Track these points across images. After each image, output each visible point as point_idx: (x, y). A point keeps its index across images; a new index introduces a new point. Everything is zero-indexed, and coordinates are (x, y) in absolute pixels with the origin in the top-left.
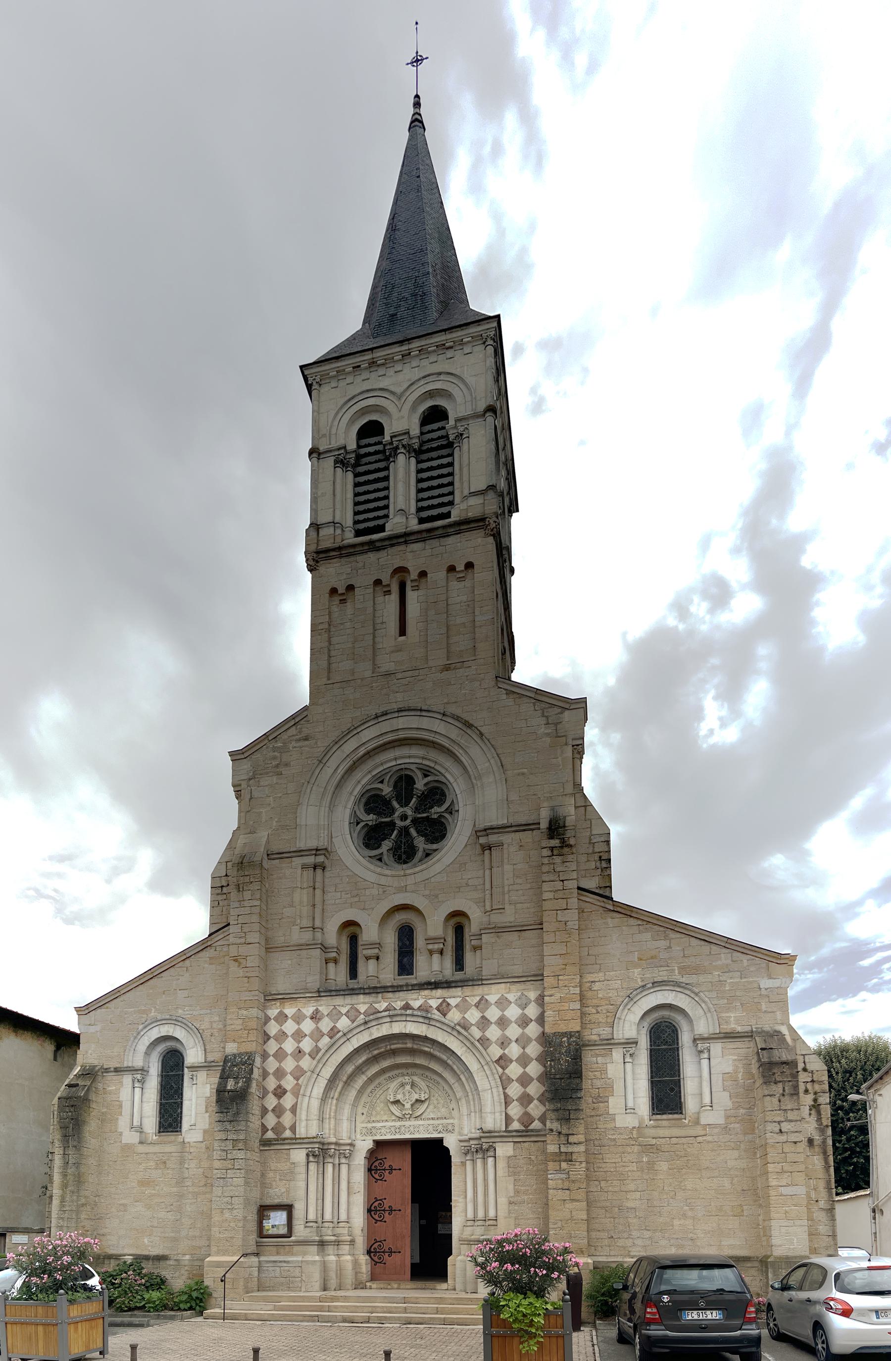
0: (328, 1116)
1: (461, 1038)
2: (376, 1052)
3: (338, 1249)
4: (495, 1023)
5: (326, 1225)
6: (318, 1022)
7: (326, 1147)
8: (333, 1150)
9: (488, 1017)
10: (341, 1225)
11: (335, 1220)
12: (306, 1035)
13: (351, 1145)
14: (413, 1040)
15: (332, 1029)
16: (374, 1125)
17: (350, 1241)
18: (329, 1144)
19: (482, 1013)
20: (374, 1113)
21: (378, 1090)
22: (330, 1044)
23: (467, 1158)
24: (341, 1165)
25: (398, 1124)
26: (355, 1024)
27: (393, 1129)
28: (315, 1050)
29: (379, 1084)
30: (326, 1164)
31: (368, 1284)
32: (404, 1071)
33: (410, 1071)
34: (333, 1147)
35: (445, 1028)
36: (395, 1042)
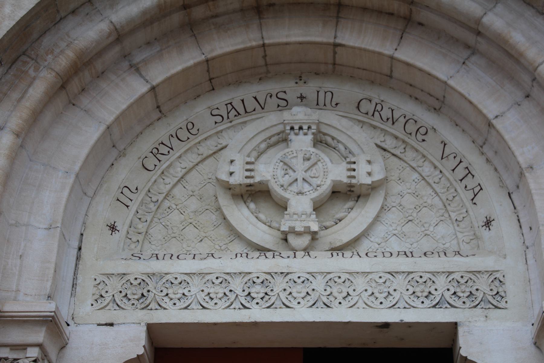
16: (156, 266)
20: (157, 232)
21: (180, 148)
27: (237, 285)
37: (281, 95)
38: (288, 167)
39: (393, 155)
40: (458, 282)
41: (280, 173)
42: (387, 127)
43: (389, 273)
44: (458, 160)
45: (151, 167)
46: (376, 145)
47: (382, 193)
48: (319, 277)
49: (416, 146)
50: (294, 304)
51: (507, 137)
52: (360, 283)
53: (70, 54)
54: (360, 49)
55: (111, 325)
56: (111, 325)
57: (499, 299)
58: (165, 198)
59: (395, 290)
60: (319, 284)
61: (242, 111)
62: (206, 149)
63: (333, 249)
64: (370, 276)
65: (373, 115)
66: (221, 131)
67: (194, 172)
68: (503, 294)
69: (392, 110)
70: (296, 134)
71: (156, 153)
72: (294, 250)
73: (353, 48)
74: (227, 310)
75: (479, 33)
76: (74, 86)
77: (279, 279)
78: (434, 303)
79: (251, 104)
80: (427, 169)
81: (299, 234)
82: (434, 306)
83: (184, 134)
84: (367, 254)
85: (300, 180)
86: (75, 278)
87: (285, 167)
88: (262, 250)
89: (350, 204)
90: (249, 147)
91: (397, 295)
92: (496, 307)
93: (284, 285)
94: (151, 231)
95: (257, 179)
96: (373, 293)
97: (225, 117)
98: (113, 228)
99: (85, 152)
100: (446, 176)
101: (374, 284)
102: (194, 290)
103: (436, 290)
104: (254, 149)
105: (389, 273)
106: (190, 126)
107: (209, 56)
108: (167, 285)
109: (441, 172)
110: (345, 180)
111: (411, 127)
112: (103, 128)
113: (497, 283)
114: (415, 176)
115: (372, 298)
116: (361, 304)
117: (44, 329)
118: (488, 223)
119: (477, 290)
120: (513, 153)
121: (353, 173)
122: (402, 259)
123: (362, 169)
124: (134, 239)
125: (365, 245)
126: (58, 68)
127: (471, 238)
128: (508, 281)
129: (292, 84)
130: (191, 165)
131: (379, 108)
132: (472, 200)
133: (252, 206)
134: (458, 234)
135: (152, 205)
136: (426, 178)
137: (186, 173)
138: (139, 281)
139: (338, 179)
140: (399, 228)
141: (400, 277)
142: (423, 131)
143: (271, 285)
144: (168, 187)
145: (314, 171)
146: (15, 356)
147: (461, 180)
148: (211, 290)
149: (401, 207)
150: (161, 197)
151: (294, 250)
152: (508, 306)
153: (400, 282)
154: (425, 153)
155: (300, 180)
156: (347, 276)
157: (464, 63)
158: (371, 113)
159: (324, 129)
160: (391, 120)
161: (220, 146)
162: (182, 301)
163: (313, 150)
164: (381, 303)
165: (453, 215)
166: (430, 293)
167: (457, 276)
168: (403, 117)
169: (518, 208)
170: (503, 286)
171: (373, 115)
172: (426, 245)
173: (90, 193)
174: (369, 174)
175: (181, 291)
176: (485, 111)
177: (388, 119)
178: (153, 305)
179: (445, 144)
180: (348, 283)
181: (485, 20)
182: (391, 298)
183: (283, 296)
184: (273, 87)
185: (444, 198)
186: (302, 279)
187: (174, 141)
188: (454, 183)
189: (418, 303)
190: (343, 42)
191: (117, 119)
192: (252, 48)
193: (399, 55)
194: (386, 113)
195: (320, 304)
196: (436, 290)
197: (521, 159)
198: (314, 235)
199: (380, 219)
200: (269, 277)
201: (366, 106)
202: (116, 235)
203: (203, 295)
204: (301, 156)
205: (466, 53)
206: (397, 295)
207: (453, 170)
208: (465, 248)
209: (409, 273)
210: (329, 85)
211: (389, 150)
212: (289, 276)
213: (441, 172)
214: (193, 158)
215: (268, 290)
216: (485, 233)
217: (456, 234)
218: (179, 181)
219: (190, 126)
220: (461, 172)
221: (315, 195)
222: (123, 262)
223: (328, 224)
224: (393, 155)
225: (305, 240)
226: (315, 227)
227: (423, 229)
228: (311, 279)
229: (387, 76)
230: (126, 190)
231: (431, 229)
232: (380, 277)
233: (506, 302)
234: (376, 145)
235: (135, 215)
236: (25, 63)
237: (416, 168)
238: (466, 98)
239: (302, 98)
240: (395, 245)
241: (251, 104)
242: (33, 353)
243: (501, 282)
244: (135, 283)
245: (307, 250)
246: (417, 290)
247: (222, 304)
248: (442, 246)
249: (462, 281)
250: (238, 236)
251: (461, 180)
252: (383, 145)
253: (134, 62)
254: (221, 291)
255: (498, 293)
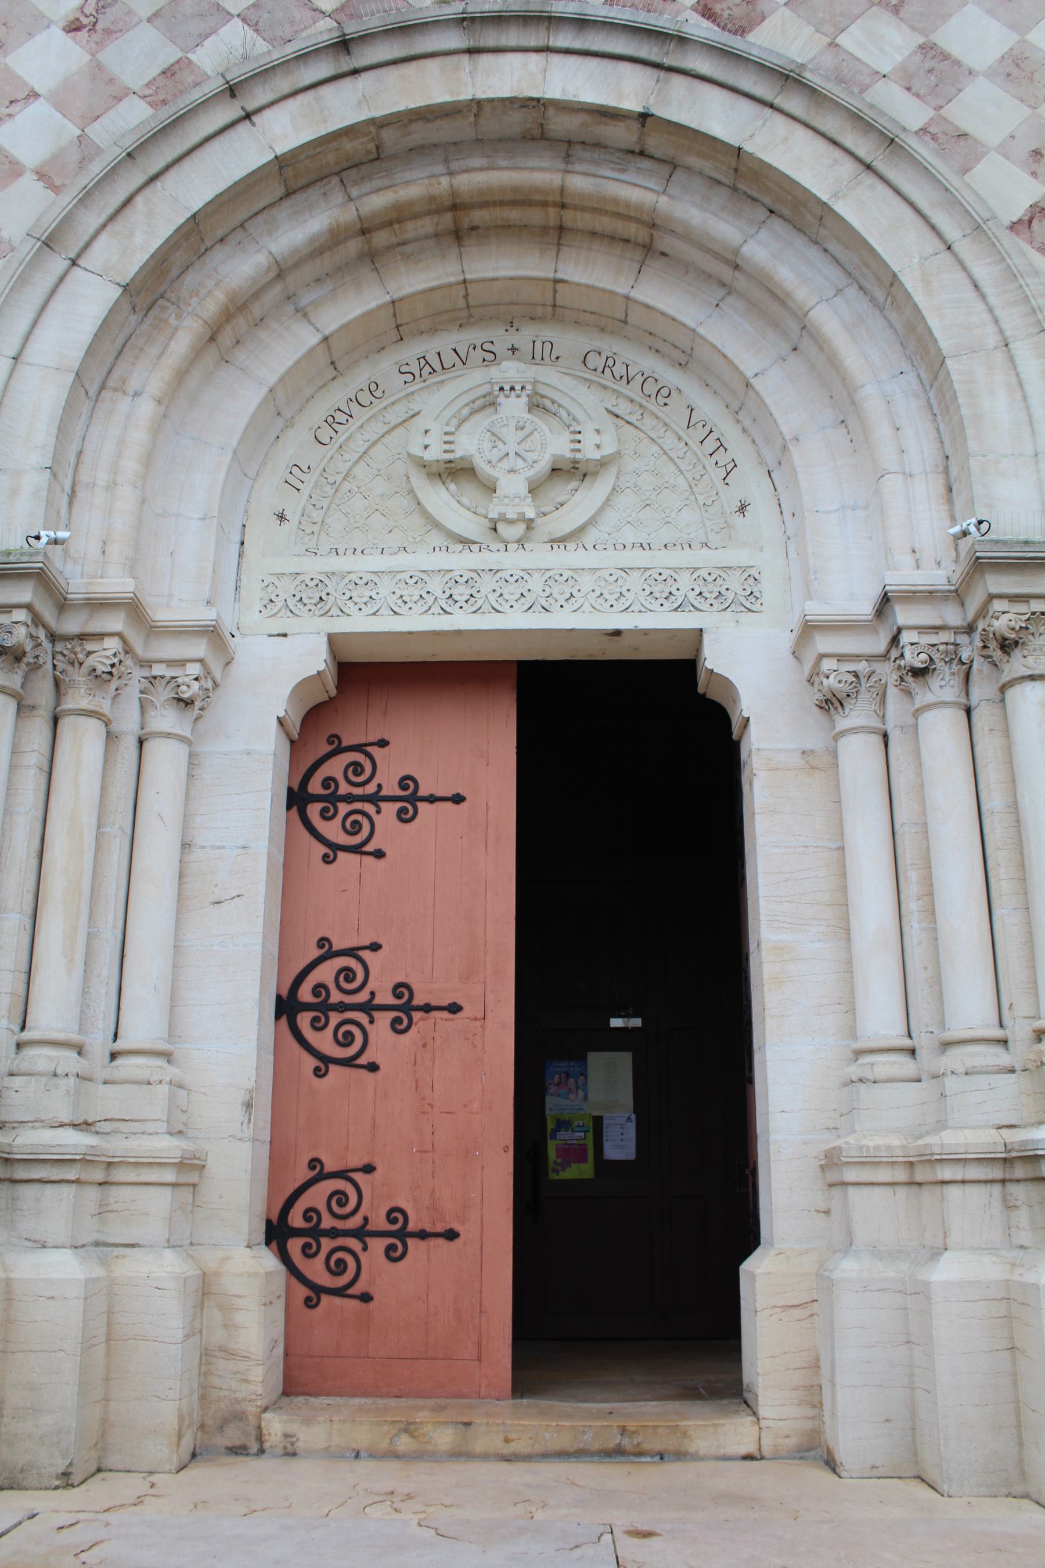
0: (103, 477)
1: (830, 123)
2: (377, 202)
3: (103, 1211)
4: (991, 74)
5: (40, 1058)
6: (100, 44)
7: (72, 625)
8: (112, 644)
9: (955, 50)
10: (127, 1066)
11: (98, 1041)
12: (34, 95)
13: (213, 633)
14: (567, 157)
15: (168, 72)
17: (182, 1166)
18: (98, 605)
19: (923, 32)
21: (361, 415)
22: (155, 125)
23: (843, 723)
24: (149, 746)
25: (461, 561)
26: (290, 49)
27: (436, 585)
28: (73, 155)
29: (373, 388)
30: (65, 724)
31: (275, 1425)
32: (501, 338)
33: (524, 337)
34: (115, 622)
35: (747, 82)
36: (478, 162)
37: (486, 347)
38: (496, 437)
39: (628, 422)
40: (705, 580)
41: (487, 445)
42: (621, 386)
43: (621, 569)
44: (707, 429)
45: (326, 440)
46: (606, 409)
47: (614, 469)
48: (536, 575)
49: (656, 411)
50: (505, 607)
51: (768, 401)
52: (586, 582)
53: (221, 296)
54: (588, 286)
55: (285, 635)
56: (285, 635)
57: (753, 600)
58: (344, 479)
59: (628, 590)
60: (536, 583)
61: (437, 366)
62: (394, 416)
63: (553, 541)
64: (598, 573)
65: (603, 372)
66: (413, 393)
67: (379, 446)
68: (758, 595)
69: (627, 366)
70: (507, 396)
71: (331, 422)
72: (506, 543)
73: (579, 285)
74: (425, 616)
75: (737, 267)
76: (227, 337)
77: (487, 577)
78: (676, 605)
79: (449, 358)
80: (669, 441)
81: (511, 522)
82: (676, 610)
83: (365, 398)
84: (594, 547)
85: (512, 454)
86: (238, 580)
87: (493, 438)
88: (465, 542)
89: (574, 484)
90: (448, 413)
91: (630, 596)
92: (749, 610)
93: (494, 586)
94: (328, 521)
95: (458, 454)
96: (602, 594)
97: (417, 375)
98: (281, 517)
99: (242, 422)
100: (692, 450)
101: (603, 583)
102: (384, 592)
103: (678, 590)
104: (454, 416)
105: (621, 569)
106: (373, 387)
107: (396, 296)
108: (351, 587)
109: (686, 444)
110: (569, 455)
111: (651, 388)
112: (264, 391)
113: (751, 581)
114: (656, 449)
115: (601, 600)
116: (587, 608)
117: (205, 641)
118: (742, 508)
119: (727, 589)
120: (775, 421)
121: (578, 446)
122: (638, 552)
123: (589, 440)
124: (308, 531)
125: (592, 535)
126: (205, 315)
127: (722, 526)
128: (762, 578)
129: (501, 331)
130: (376, 437)
131: (610, 362)
132: (724, 479)
133: (453, 487)
134: (706, 521)
135: (328, 488)
136: (668, 451)
137: (370, 448)
138: (315, 582)
139: (560, 453)
140: (634, 515)
141: (635, 574)
142: (665, 392)
143: (477, 585)
144: (348, 465)
145: (529, 443)
146: (174, 674)
147: (711, 455)
148: (405, 593)
149: (637, 488)
150: (339, 478)
151: (506, 543)
152: (762, 608)
153: (634, 580)
154: (667, 420)
155: (512, 454)
156: (571, 573)
157: (717, 305)
158: (600, 369)
159: (543, 390)
160: (625, 378)
161: (411, 413)
162: (369, 605)
163: (529, 416)
164: (612, 606)
165: (700, 498)
166: (670, 593)
167: (703, 573)
168: (640, 374)
169: (778, 490)
170: (759, 585)
171: (603, 372)
172: (667, 535)
173: (252, 474)
174: (598, 446)
175: (368, 594)
176: (742, 368)
177: (621, 377)
178: (335, 611)
179: (692, 410)
180: (571, 582)
181: (745, 250)
182: (623, 599)
183: (492, 598)
184: (475, 335)
185: (690, 477)
186: (515, 578)
187: (355, 408)
188: (702, 458)
189: (655, 606)
190: (565, 277)
191: (282, 379)
192: (450, 285)
193: (635, 294)
194: (619, 370)
195: (537, 607)
196: (678, 590)
197: (784, 429)
198: (530, 524)
199: (610, 503)
200: (474, 575)
201: (594, 361)
202: (286, 525)
203: (395, 597)
204: (513, 424)
205: (720, 293)
206: (630, 596)
207: (702, 442)
208: (714, 540)
209: (646, 569)
210: (548, 332)
211: (623, 416)
212: (500, 574)
213: (686, 444)
214: (377, 428)
215: (474, 592)
216: (738, 519)
217: (703, 522)
218: (361, 457)
219: (373, 387)
220: (711, 444)
221: (531, 473)
222: (296, 559)
223: (546, 509)
224: (628, 422)
225: (520, 529)
226: (530, 514)
227: (664, 515)
228: (526, 577)
229: (621, 321)
230: (295, 470)
231: (673, 515)
232: (611, 575)
233: (762, 604)
234: (606, 409)
235: (308, 500)
236: (164, 309)
237: (656, 440)
238: (719, 351)
239: (513, 349)
240: (629, 536)
241: (449, 358)
242: (194, 669)
243: (756, 580)
244: (311, 584)
245: (521, 542)
246: (655, 589)
247: (419, 608)
248: (685, 536)
249: (710, 579)
250: (437, 525)
251: (711, 455)
252: (615, 410)
253: (302, 304)
254: (416, 592)
255: (752, 593)
